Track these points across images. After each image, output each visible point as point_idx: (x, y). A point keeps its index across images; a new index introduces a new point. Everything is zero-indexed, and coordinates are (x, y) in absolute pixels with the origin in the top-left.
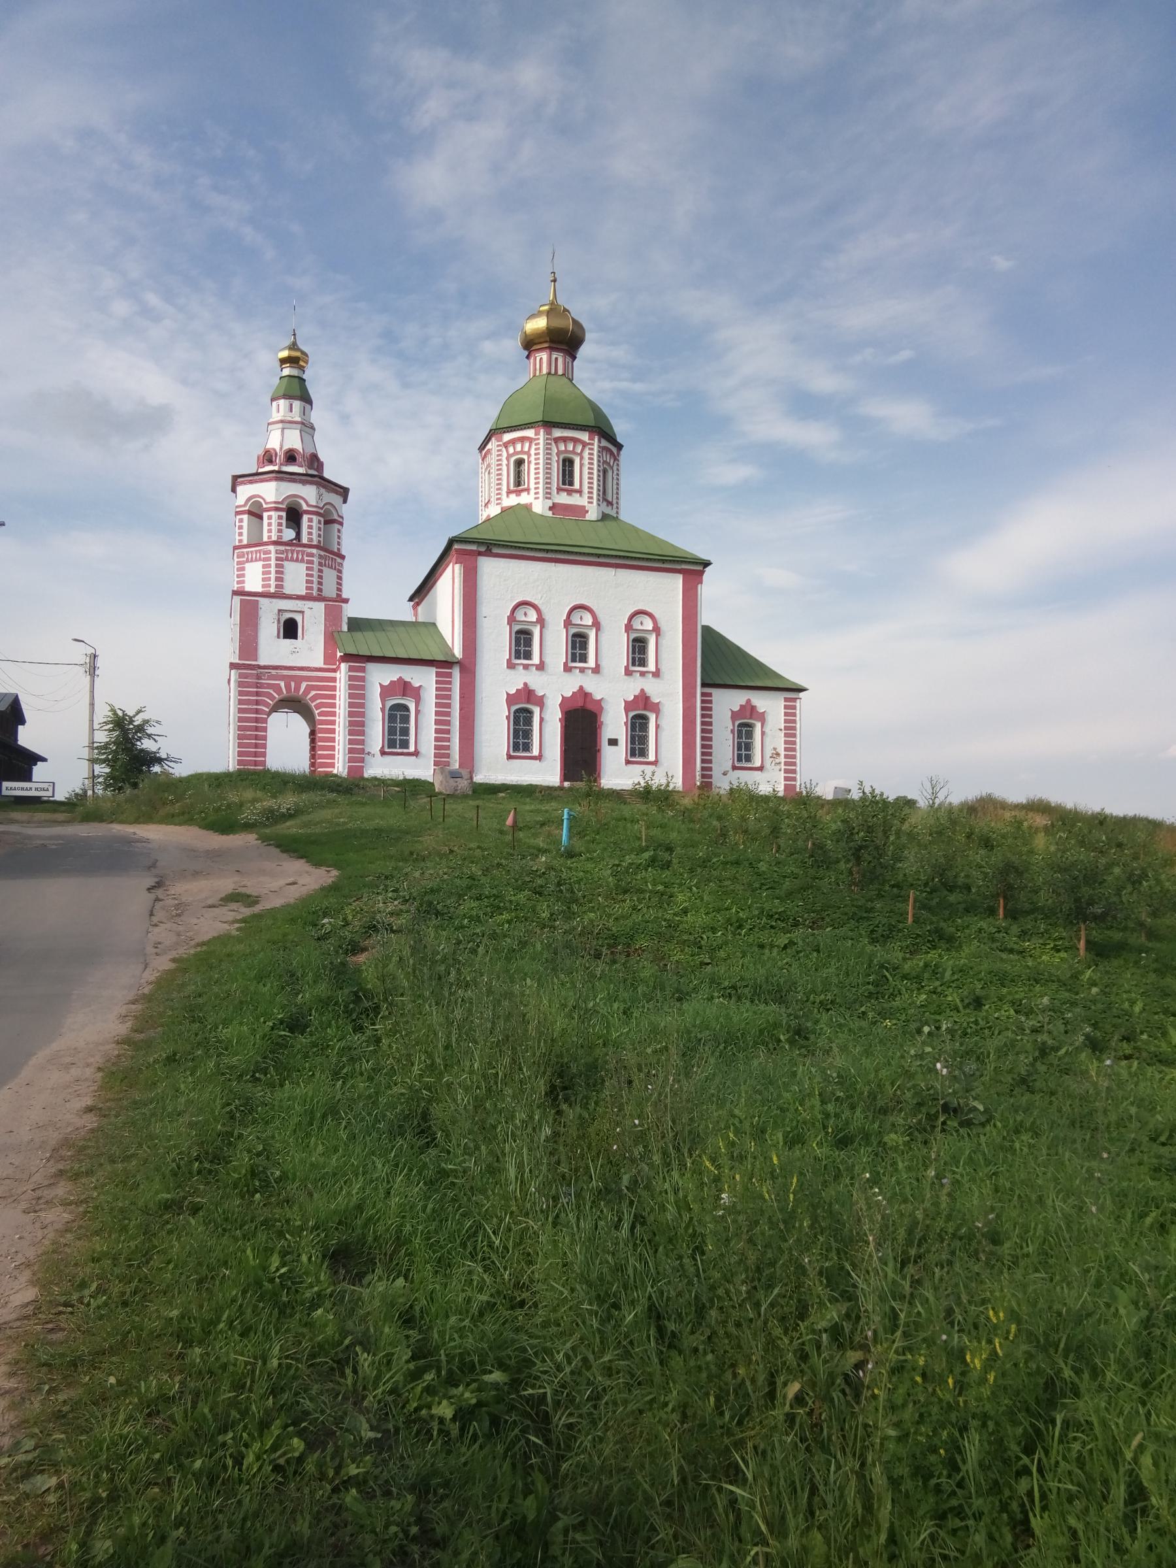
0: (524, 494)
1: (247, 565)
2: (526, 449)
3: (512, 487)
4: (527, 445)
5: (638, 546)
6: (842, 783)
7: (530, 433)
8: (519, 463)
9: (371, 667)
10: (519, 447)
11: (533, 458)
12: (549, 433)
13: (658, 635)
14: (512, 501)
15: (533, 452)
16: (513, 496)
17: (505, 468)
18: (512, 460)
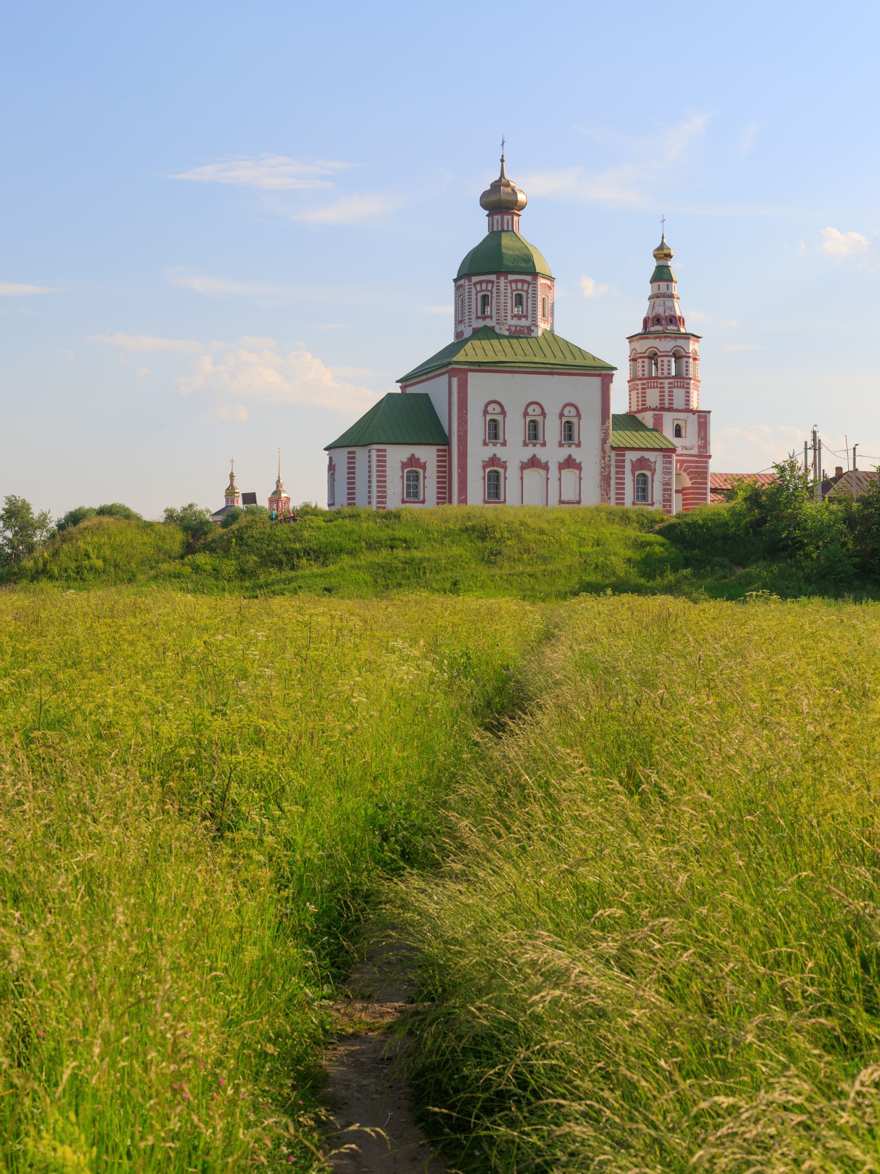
0: (488, 320)
1: (647, 391)
2: (489, 288)
3: (479, 314)
4: (490, 286)
5: (579, 362)
6: (308, 501)
7: (493, 277)
8: (485, 298)
9: (627, 453)
10: (484, 286)
11: (494, 295)
12: (506, 278)
13: (505, 416)
14: (480, 324)
15: (494, 291)
16: (480, 321)
17: (474, 301)
18: (480, 295)
